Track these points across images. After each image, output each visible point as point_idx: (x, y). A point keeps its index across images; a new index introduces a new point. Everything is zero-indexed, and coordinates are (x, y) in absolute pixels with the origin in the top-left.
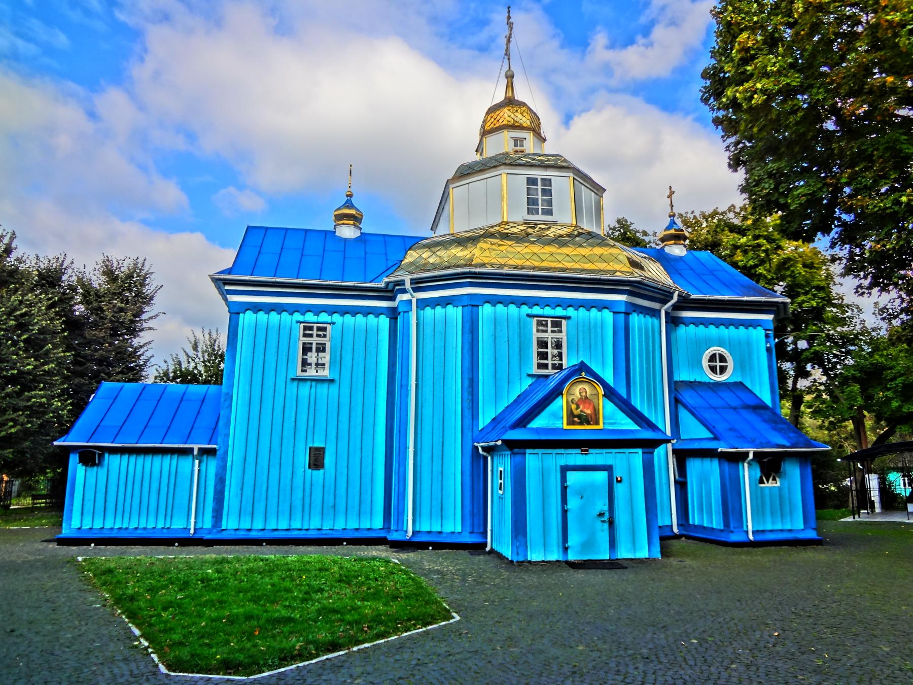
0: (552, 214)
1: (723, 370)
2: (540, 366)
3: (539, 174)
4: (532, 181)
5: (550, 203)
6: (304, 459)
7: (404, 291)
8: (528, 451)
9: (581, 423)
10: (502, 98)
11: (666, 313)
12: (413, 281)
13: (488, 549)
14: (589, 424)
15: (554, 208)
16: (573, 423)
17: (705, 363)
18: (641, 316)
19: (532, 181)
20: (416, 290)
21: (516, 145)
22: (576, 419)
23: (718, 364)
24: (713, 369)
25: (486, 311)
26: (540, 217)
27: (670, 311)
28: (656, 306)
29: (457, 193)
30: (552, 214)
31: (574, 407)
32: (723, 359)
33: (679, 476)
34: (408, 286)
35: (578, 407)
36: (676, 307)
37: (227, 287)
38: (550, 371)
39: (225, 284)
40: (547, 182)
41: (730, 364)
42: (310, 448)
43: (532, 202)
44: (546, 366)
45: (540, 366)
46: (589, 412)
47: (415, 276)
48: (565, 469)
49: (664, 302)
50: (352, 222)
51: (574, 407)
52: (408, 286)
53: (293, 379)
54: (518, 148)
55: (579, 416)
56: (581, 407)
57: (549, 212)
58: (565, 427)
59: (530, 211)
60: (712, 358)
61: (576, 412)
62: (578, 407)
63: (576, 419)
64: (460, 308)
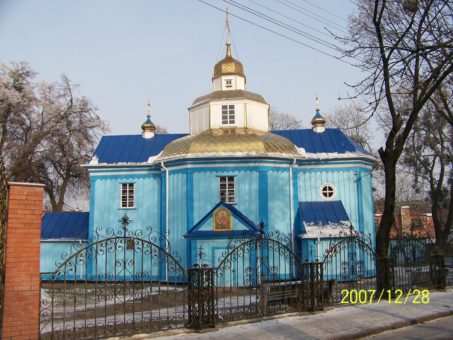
0: (234, 123)
1: (331, 194)
3: (228, 103)
4: (224, 107)
5: (233, 117)
8: (198, 241)
9: (222, 228)
10: (224, 57)
15: (236, 120)
16: (218, 228)
17: (321, 192)
19: (224, 107)
22: (219, 226)
23: (328, 192)
24: (325, 195)
25: (196, 176)
30: (234, 123)
31: (218, 221)
32: (330, 189)
35: (220, 221)
40: (232, 107)
41: (335, 192)
46: (225, 223)
48: (214, 248)
51: (218, 221)
54: (229, 85)
55: (221, 225)
57: (233, 122)
58: (215, 230)
59: (224, 123)
60: (325, 189)
61: (219, 223)
62: (220, 221)
63: (219, 226)
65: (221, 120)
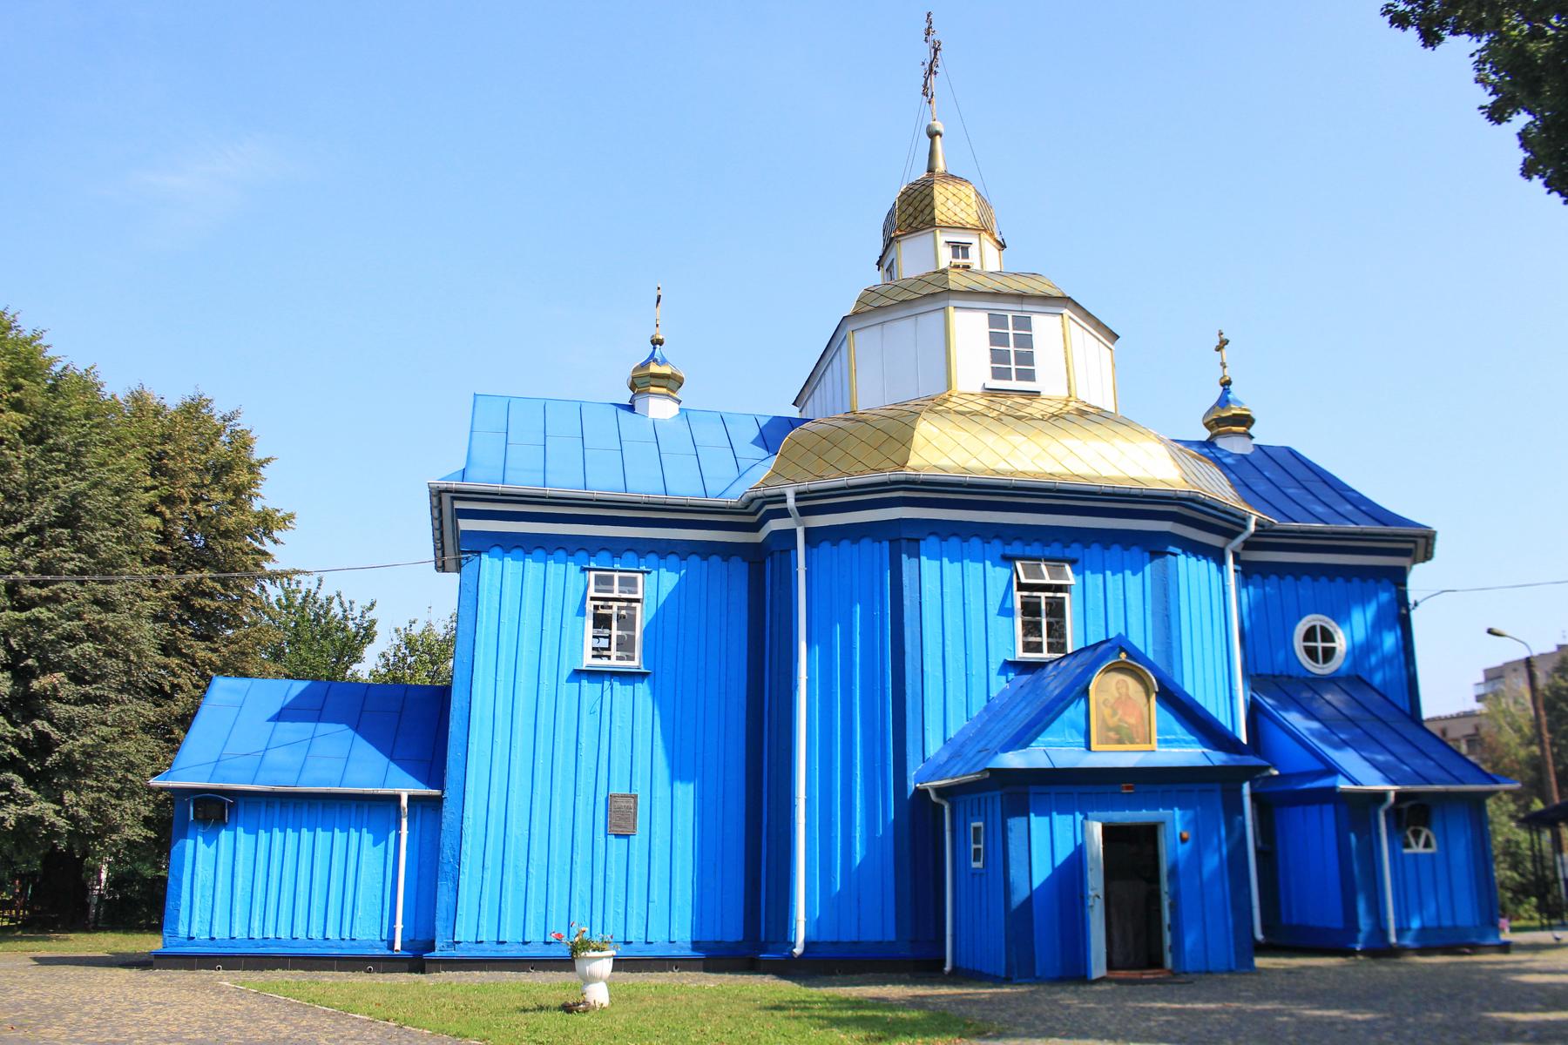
2: (1028, 647)
5: (1026, 358)
6: (591, 817)
7: (784, 513)
8: (1032, 789)
11: (1236, 555)
12: (799, 496)
13: (948, 968)
14: (1132, 742)
15: (1039, 366)
17: (1299, 644)
18: (1193, 560)
20: (804, 512)
21: (955, 256)
22: (1112, 734)
24: (1311, 653)
26: (1014, 384)
27: (1238, 550)
28: (1215, 540)
29: (864, 342)
33: (1264, 842)
34: (791, 503)
35: (1114, 714)
36: (1248, 545)
37: (459, 505)
38: (1045, 655)
39: (454, 498)
42: (610, 799)
43: (998, 357)
44: (1037, 648)
45: (1028, 647)
46: (1132, 721)
47: (802, 488)
49: (1232, 535)
50: (664, 390)
51: (1107, 712)
52: (791, 503)
53: (578, 674)
54: (961, 261)
55: (1117, 730)
56: (1120, 712)
57: (1028, 376)
59: (998, 374)
60: (1310, 635)
61: (1113, 722)
62: (1114, 714)
64: (886, 544)
65: (985, 365)
